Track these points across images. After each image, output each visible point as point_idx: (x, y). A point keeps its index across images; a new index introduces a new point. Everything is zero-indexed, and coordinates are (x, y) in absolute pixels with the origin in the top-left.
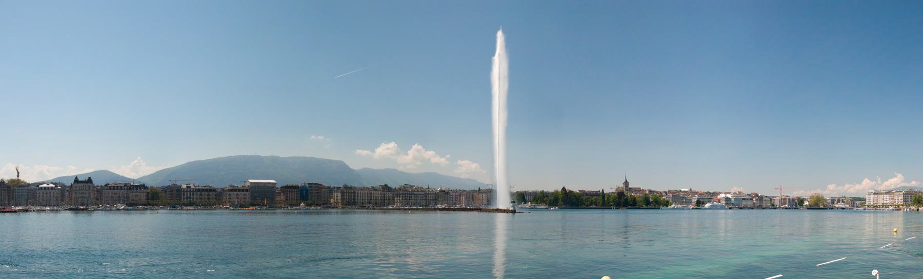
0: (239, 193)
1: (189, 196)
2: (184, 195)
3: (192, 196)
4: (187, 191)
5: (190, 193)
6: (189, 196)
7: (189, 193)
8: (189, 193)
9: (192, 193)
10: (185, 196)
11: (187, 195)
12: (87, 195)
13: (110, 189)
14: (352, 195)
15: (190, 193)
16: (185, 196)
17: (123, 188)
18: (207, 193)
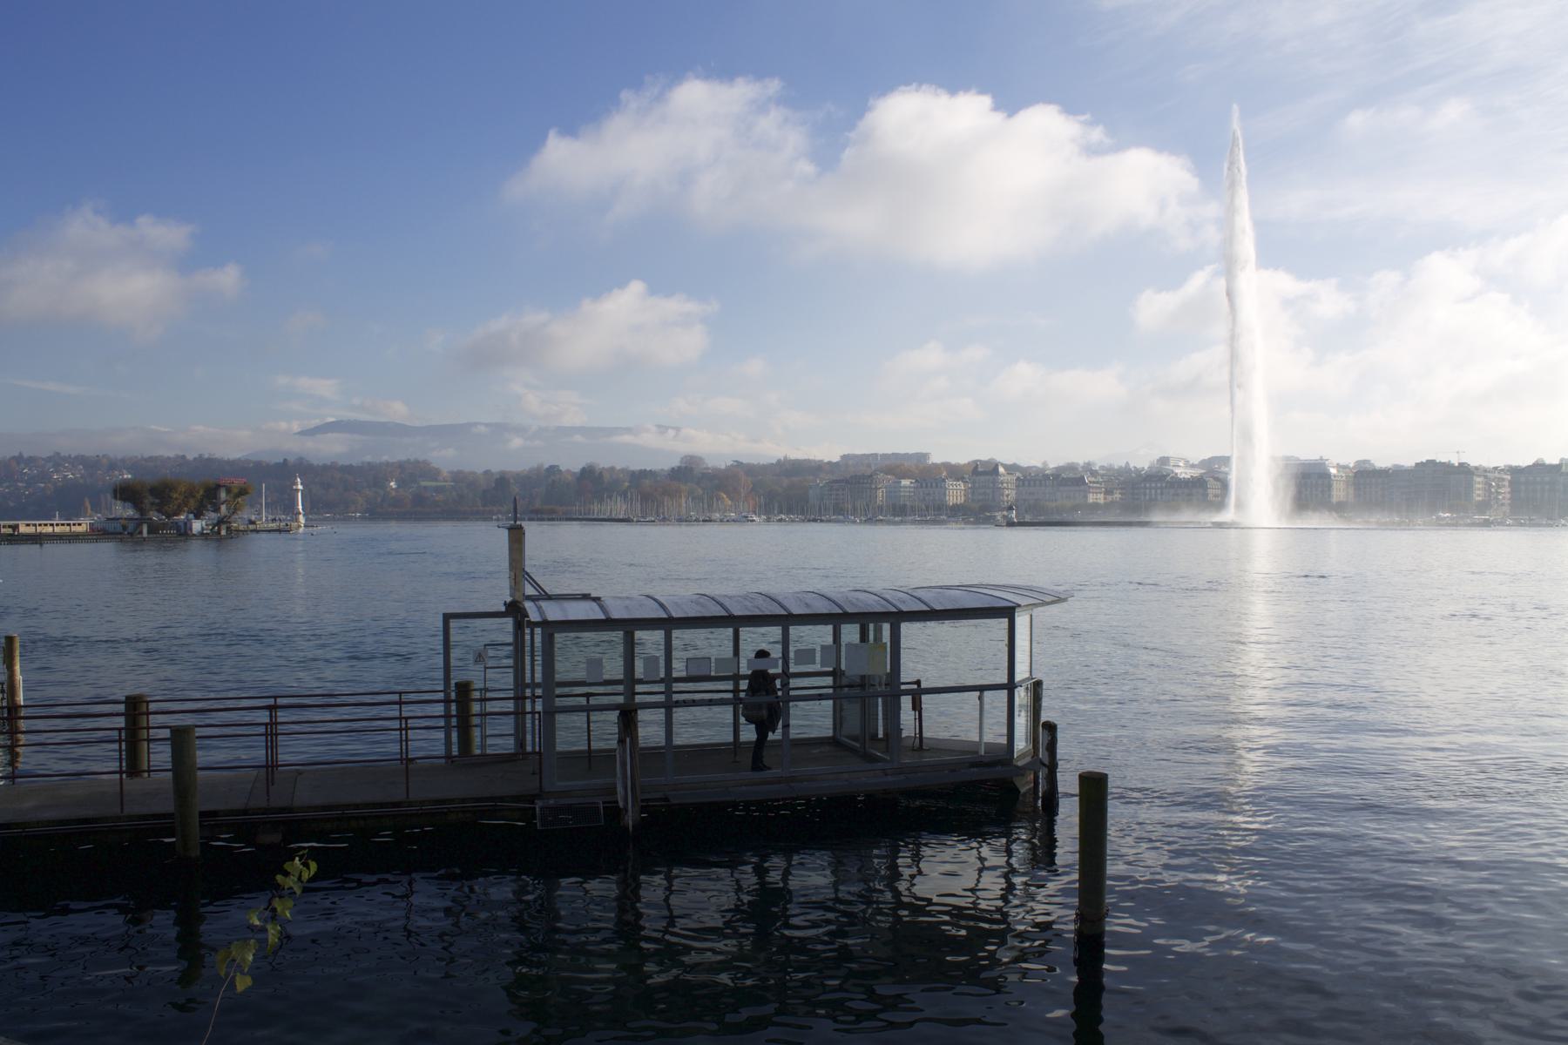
1: (1153, 496)
2: (1145, 495)
3: (1159, 497)
4: (1150, 488)
6: (1153, 496)
7: (1153, 491)
8: (1153, 491)
10: (1147, 497)
14: (1547, 487)
16: (1147, 497)
17: (1043, 482)
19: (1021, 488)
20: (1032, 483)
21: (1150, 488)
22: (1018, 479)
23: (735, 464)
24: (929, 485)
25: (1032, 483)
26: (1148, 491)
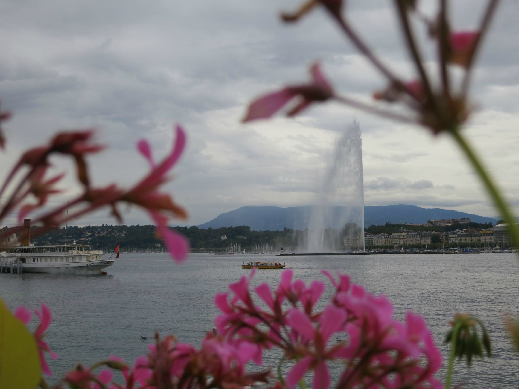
0: (487, 237)
1: (453, 241)
3: (455, 241)
4: (452, 238)
5: (454, 239)
6: (453, 241)
7: (453, 238)
8: (453, 238)
9: (455, 238)
10: (451, 241)
11: (452, 241)
12: (399, 242)
13: (409, 237)
15: (454, 239)
16: (451, 241)
17: (416, 235)
18: (464, 238)
19: (408, 238)
20: (412, 236)
21: (452, 238)
22: (407, 235)
23: (372, 226)
24: (379, 237)
25: (412, 236)
26: (451, 238)
